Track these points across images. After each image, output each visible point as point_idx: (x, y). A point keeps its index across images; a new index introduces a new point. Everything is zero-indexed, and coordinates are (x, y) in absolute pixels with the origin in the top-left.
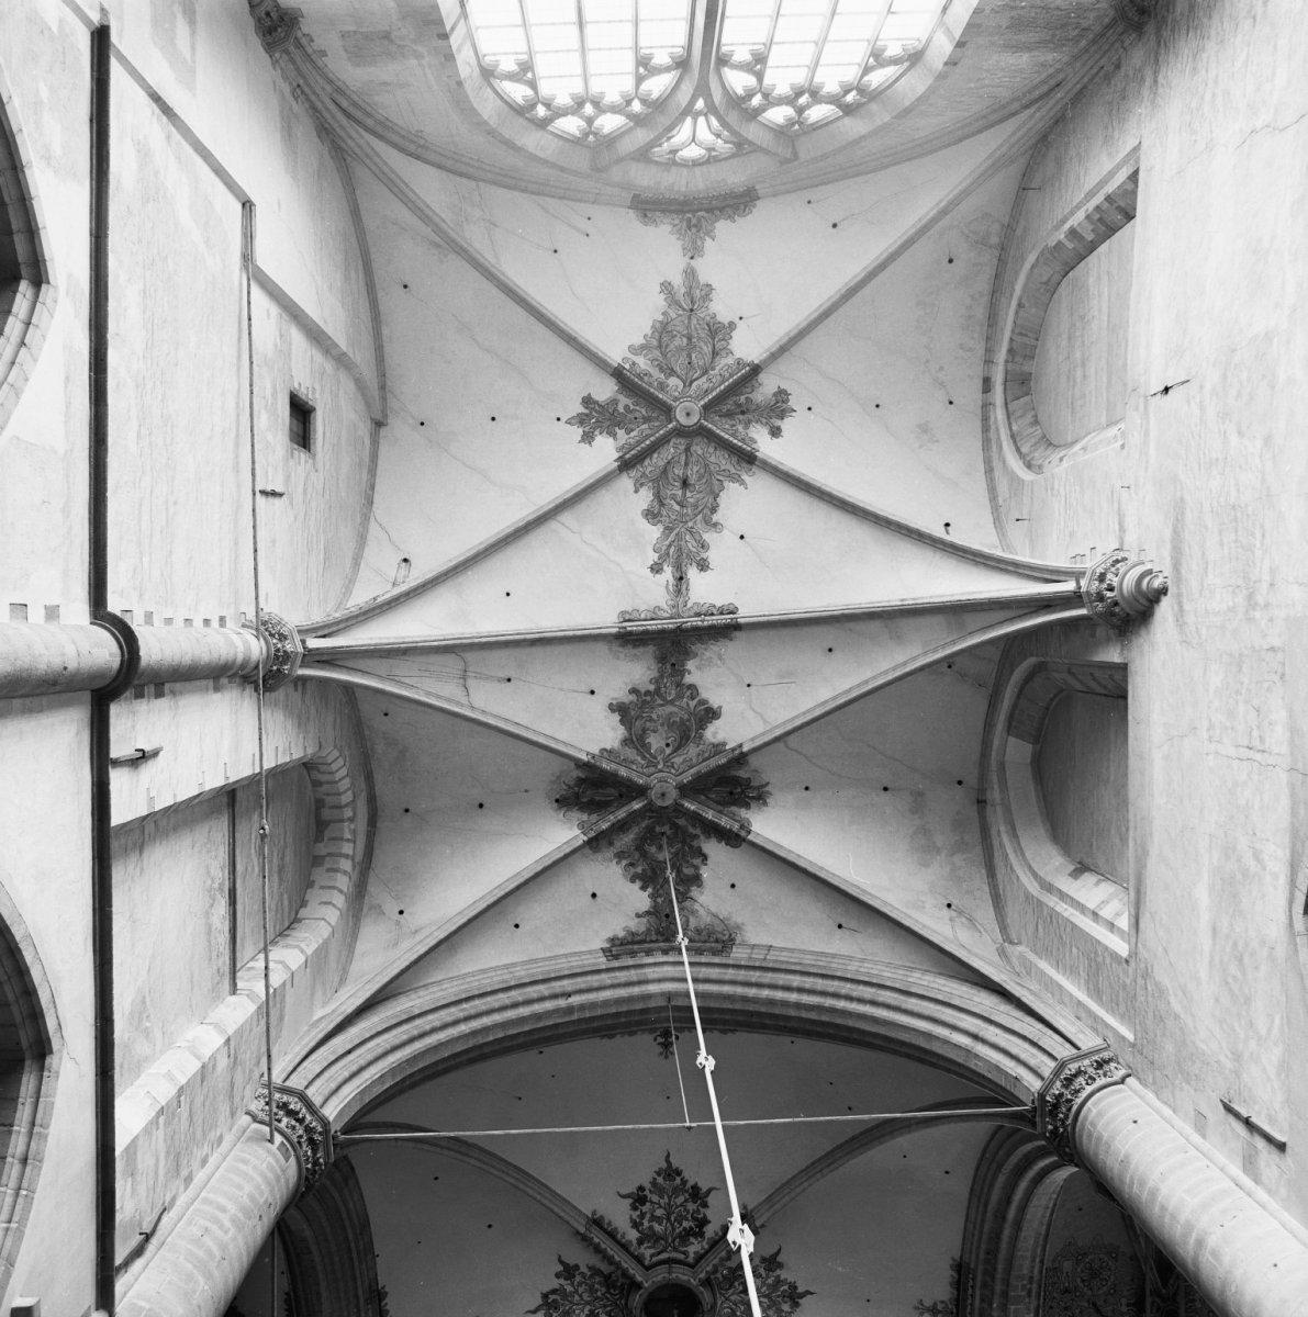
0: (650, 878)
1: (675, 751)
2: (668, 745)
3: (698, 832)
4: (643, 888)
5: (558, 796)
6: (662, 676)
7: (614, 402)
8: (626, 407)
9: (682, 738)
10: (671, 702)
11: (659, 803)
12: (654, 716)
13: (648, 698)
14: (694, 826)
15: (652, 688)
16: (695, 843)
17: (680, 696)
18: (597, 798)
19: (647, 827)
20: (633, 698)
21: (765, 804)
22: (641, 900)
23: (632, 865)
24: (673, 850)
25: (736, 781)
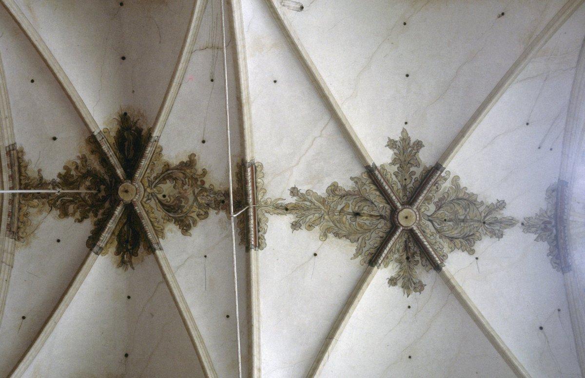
0: (66, 180)
1: (160, 201)
2: (164, 196)
3: (100, 217)
4: (60, 175)
5: (128, 114)
6: (215, 193)
7: (418, 165)
8: (413, 173)
9: (169, 206)
10: (196, 200)
11: (121, 188)
12: (186, 187)
13: (199, 183)
14: (103, 214)
15: (207, 186)
16: (91, 214)
17: (200, 206)
18: (126, 143)
19: (105, 179)
20: (200, 172)
21: (119, 266)
22: (51, 173)
23: (77, 168)
24: (87, 197)
25: (135, 246)
